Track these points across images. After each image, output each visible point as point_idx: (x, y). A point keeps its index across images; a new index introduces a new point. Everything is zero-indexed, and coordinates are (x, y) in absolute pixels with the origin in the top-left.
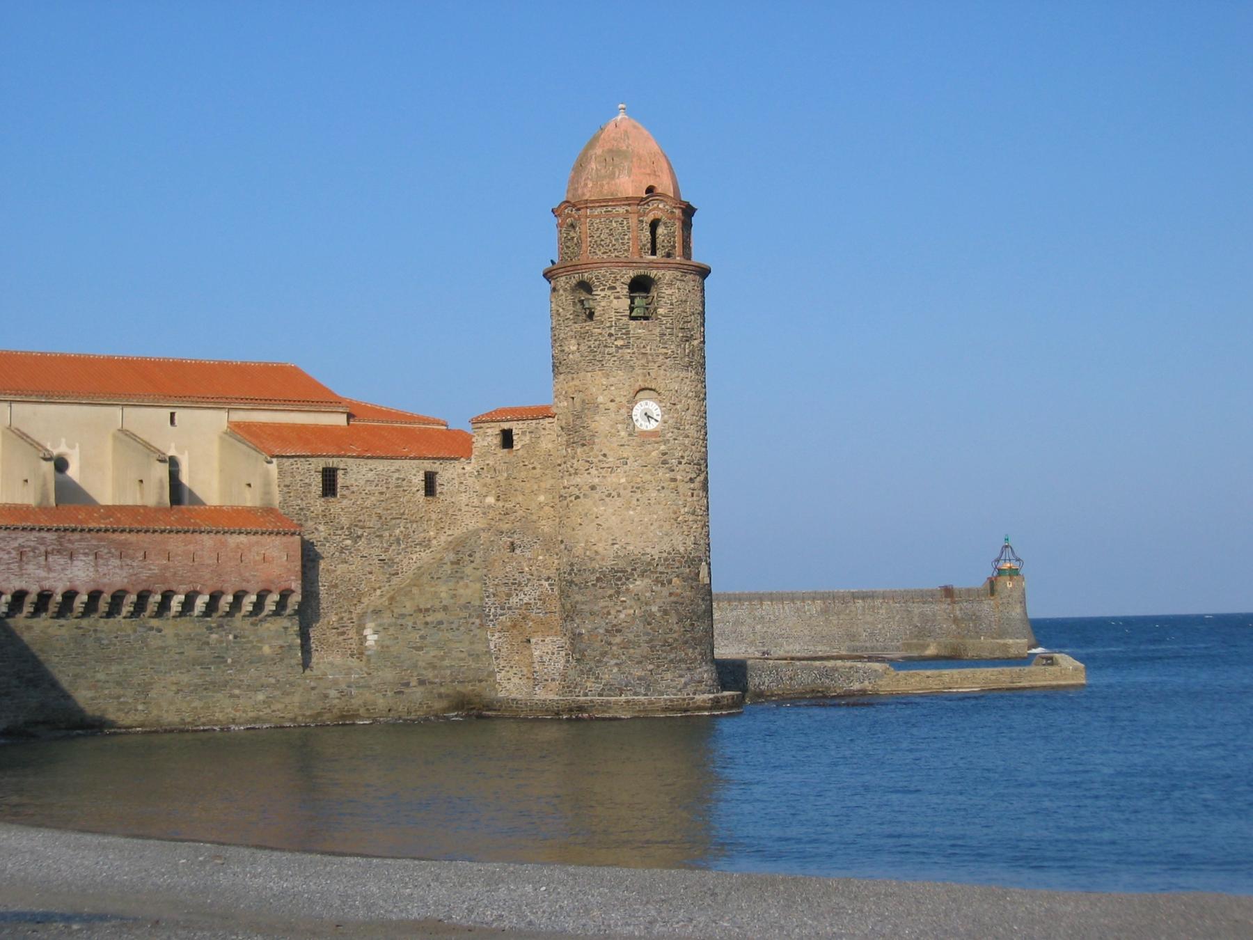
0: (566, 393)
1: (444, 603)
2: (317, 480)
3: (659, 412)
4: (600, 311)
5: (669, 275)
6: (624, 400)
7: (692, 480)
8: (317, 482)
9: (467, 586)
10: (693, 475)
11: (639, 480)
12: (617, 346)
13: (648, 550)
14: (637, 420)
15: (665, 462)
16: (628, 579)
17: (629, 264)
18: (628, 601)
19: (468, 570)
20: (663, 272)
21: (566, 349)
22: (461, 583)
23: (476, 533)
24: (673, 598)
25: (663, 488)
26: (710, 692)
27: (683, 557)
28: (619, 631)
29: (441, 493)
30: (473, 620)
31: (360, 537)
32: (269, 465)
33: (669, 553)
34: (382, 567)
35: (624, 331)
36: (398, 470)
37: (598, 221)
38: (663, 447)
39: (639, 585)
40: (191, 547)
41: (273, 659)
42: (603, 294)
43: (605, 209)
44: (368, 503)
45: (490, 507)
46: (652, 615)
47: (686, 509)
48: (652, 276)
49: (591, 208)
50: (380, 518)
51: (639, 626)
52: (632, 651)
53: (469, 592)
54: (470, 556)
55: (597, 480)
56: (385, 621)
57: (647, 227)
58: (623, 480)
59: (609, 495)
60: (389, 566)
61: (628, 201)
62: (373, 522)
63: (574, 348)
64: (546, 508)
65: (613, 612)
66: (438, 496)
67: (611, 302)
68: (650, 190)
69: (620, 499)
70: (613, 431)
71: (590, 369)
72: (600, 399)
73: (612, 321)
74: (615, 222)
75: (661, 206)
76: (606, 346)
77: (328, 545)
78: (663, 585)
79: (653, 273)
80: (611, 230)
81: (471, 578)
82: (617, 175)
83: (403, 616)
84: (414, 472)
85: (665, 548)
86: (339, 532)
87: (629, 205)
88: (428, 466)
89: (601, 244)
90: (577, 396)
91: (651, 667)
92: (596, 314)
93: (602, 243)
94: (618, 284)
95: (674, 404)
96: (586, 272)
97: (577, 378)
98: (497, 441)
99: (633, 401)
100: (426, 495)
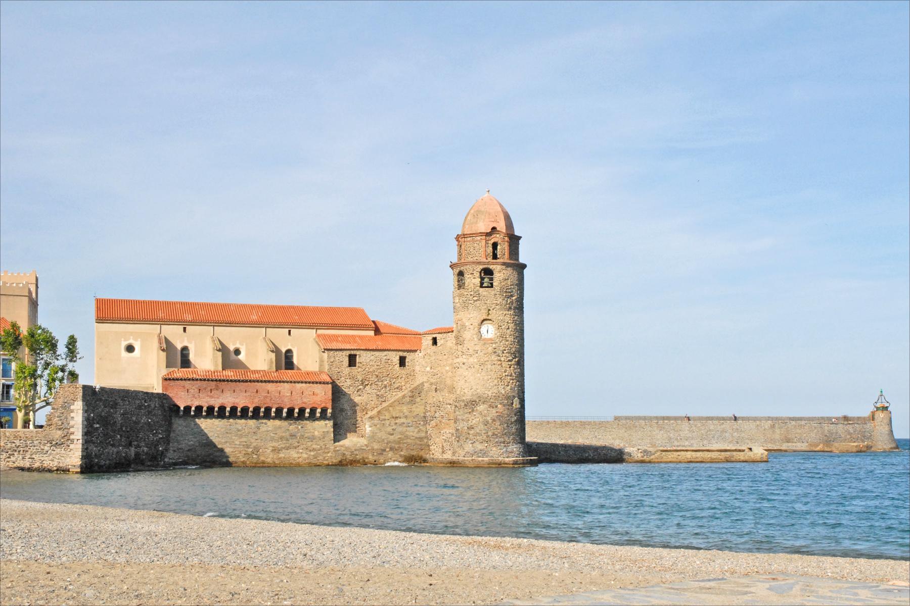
1: (406, 414)
2: (347, 359)
3: (493, 330)
5: (499, 267)
6: (476, 324)
7: (510, 361)
8: (346, 361)
9: (417, 407)
10: (511, 358)
11: (482, 360)
13: (486, 392)
14: (483, 333)
15: (495, 352)
16: (477, 405)
17: (479, 263)
18: (477, 415)
19: (418, 400)
20: (496, 266)
22: (414, 406)
23: (422, 384)
24: (497, 414)
25: (494, 364)
26: (517, 457)
27: (504, 395)
28: (473, 428)
29: (408, 366)
30: (418, 422)
31: (367, 385)
32: (323, 354)
33: (496, 394)
34: (378, 398)
35: (477, 293)
36: (386, 355)
38: (494, 345)
39: (481, 408)
40: (279, 389)
41: (319, 437)
43: (472, 238)
44: (371, 370)
45: (428, 372)
46: (487, 422)
47: (506, 374)
48: (491, 268)
49: (467, 237)
50: (377, 376)
51: (482, 427)
52: (478, 437)
53: (418, 410)
54: (419, 394)
55: (465, 361)
56: (376, 422)
57: (490, 246)
58: (475, 360)
60: (382, 398)
61: (481, 234)
62: (374, 379)
64: (450, 373)
65: (470, 419)
66: (406, 367)
68: (494, 229)
69: (474, 369)
70: (472, 338)
72: (467, 324)
75: (498, 236)
77: (351, 388)
78: (493, 408)
79: (491, 267)
81: (419, 404)
82: (478, 222)
83: (385, 420)
84: (394, 356)
85: (494, 391)
86: (357, 383)
87: (481, 236)
88: (401, 354)
90: (459, 322)
91: (486, 445)
92: (466, 285)
94: (475, 272)
95: (501, 326)
98: (431, 342)
100: (400, 366)
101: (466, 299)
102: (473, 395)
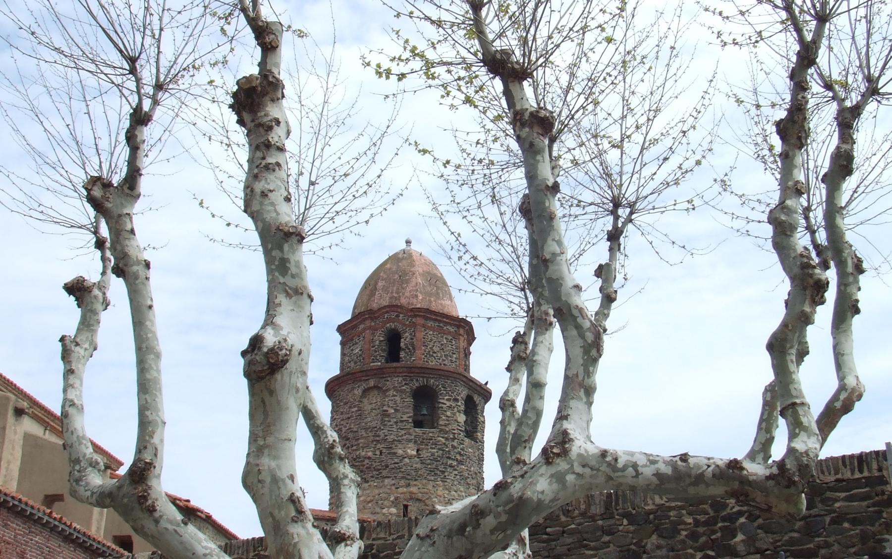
0: (396, 498)
4: (444, 420)
12: (457, 460)
21: (400, 452)
37: (431, 333)
42: (448, 405)
63: (414, 453)
67: (454, 414)
71: (433, 478)
73: (454, 433)
74: (446, 338)
76: (449, 458)
80: (442, 345)
82: (441, 295)
89: (432, 356)
93: (435, 355)
94: (459, 398)
96: (433, 378)
97: (415, 485)
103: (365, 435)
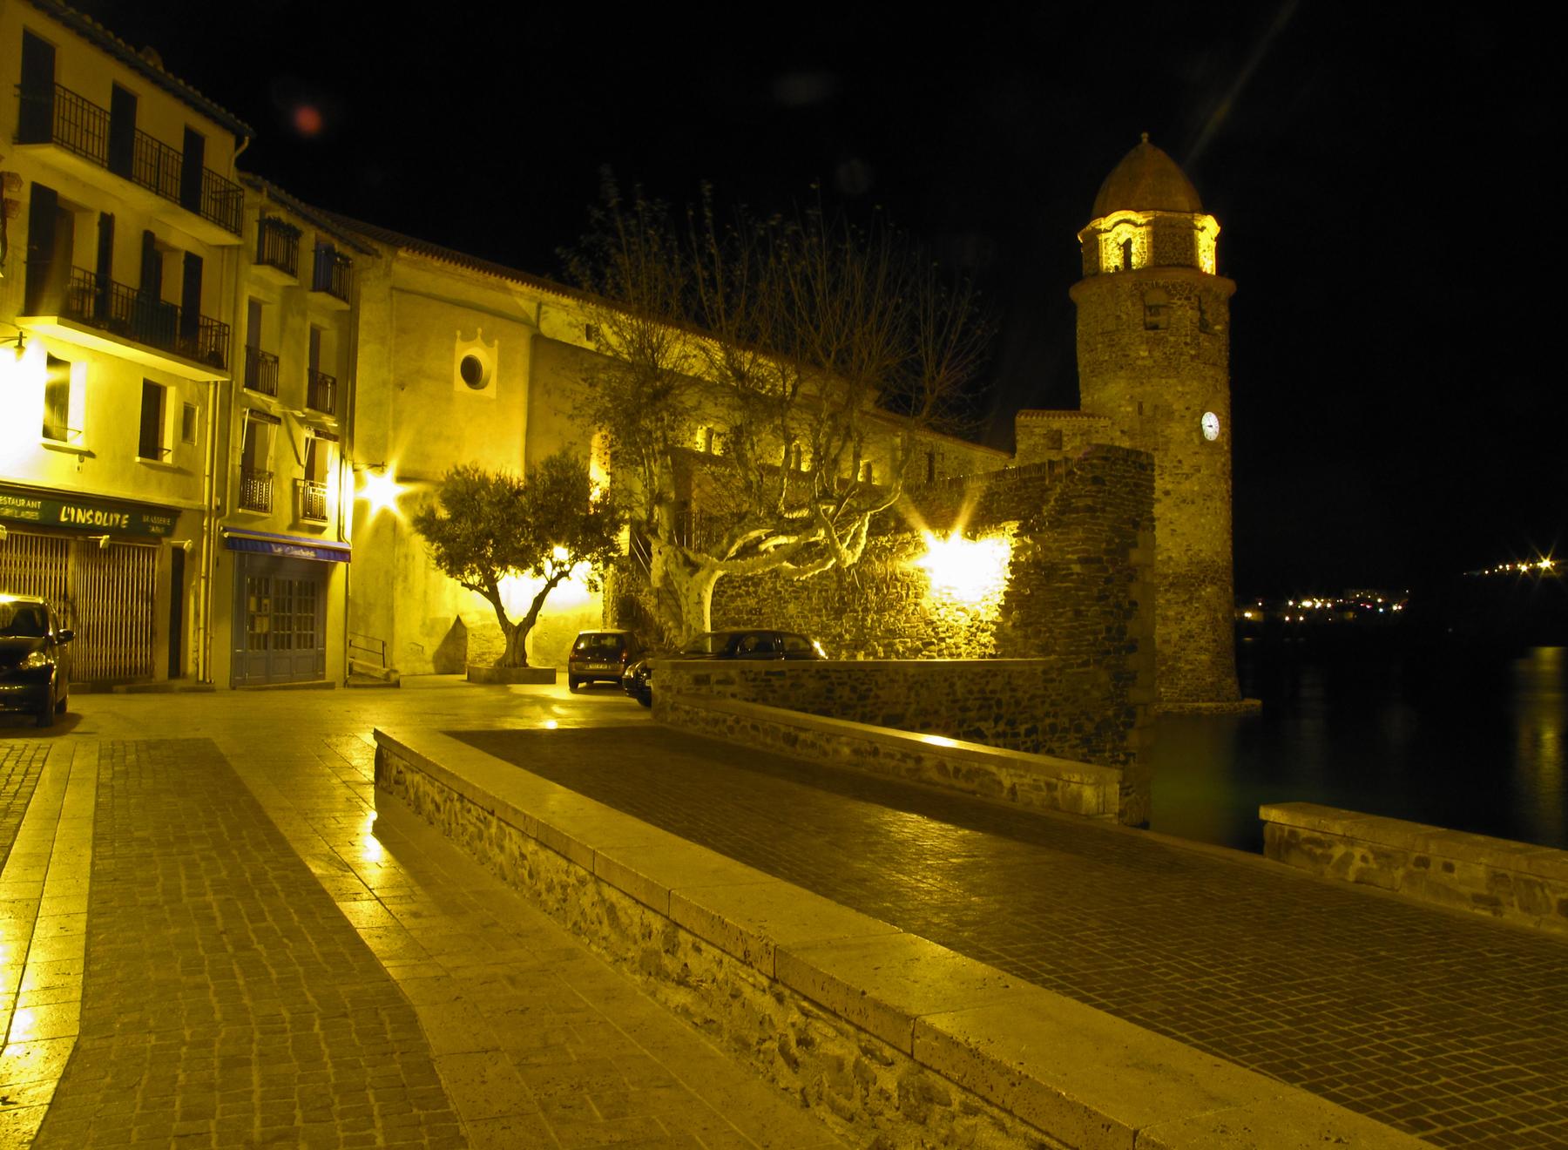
6: (1198, 408)
16: (1200, 585)
21: (1133, 354)
39: (1208, 591)
42: (1179, 303)
55: (1169, 487)
59: (1184, 501)
63: (1146, 354)
72: (1175, 407)
94: (1192, 295)
99: (1202, 413)
101: (1172, 350)
102: (1191, 563)
103: (1101, 340)
